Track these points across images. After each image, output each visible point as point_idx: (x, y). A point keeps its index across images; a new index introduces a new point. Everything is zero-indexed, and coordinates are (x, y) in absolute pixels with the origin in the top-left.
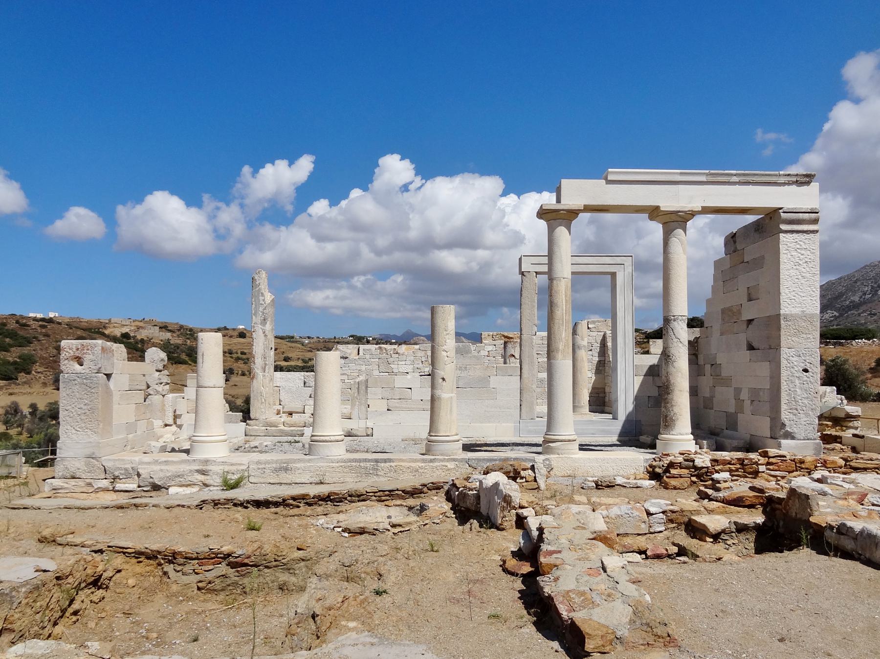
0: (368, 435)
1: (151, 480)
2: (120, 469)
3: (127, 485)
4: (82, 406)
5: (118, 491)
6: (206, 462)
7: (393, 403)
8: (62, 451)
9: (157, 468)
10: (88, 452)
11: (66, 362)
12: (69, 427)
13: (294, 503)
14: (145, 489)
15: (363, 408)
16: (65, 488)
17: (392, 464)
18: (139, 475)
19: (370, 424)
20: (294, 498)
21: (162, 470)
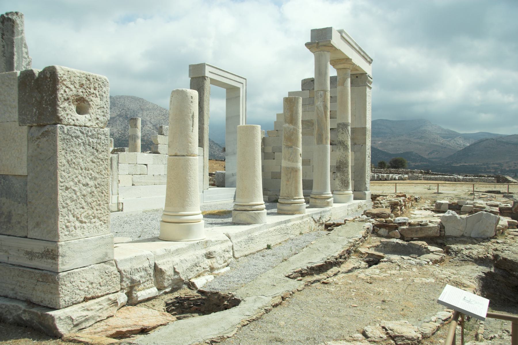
0: (119, 210)
1: (176, 277)
2: (138, 270)
3: (148, 291)
4: (88, 180)
5: (141, 302)
6: (206, 243)
7: (136, 178)
8: (66, 259)
9: (176, 259)
10: (99, 254)
11: (66, 104)
12: (71, 218)
13: (340, 260)
14: (167, 290)
15: (115, 183)
16: (93, 318)
17: (292, 223)
18: (158, 271)
19: (121, 200)
20: (341, 257)
21: (181, 261)
